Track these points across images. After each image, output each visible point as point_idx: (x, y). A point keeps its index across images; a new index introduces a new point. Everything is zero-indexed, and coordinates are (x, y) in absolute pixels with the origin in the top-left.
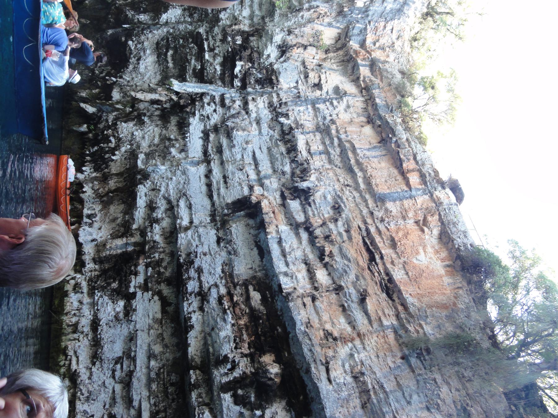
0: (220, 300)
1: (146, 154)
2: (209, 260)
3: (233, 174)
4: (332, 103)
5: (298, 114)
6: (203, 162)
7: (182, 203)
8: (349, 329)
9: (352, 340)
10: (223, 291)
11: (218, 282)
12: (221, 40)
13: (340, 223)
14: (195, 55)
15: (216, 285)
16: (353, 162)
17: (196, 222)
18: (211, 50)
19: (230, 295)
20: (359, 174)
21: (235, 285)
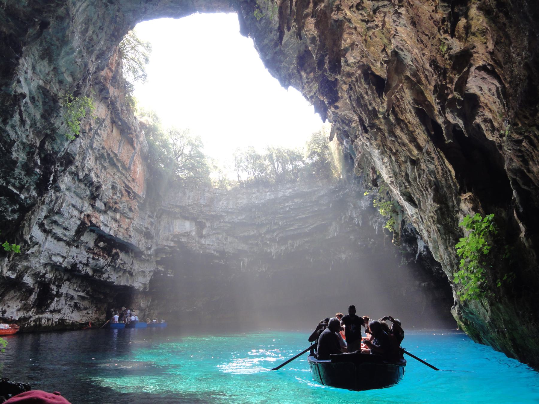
0: (93, 259)
1: (9, 270)
2: (80, 256)
3: (69, 224)
4: (98, 134)
5: (88, 163)
6: (47, 236)
7: (54, 258)
8: (129, 220)
9: (131, 222)
10: (91, 256)
11: (88, 256)
12: (25, 175)
13: (118, 194)
14: (7, 204)
15: (88, 258)
16: (115, 160)
17: (64, 255)
18: (21, 188)
19: (94, 254)
20: (119, 165)
21: (93, 250)
